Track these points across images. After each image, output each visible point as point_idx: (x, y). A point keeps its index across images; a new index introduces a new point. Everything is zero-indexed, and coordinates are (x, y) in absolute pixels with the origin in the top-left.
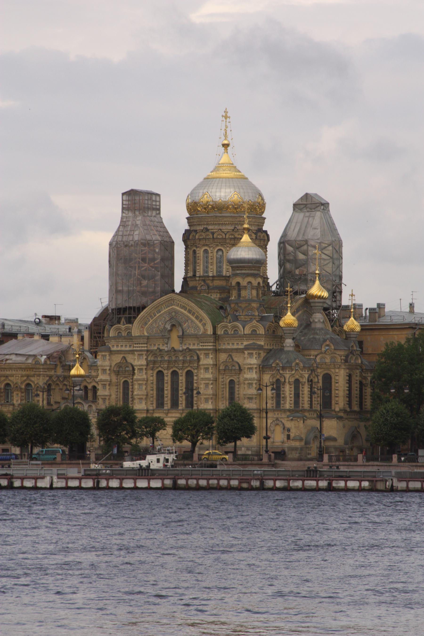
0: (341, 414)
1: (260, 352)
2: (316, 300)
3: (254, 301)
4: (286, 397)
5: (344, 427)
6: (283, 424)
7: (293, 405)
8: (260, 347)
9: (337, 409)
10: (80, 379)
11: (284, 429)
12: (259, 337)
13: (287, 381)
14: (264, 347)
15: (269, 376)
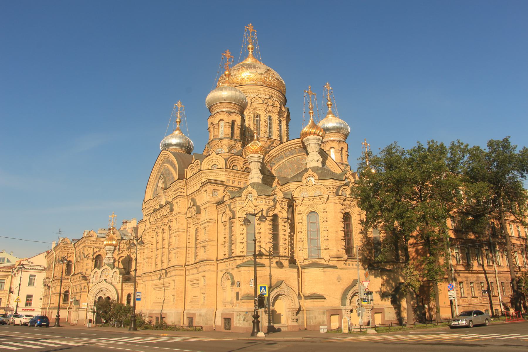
0: (333, 263)
1: (217, 188)
2: (309, 137)
3: (225, 138)
4: (236, 239)
5: (339, 279)
6: (233, 278)
7: (245, 250)
8: (220, 183)
9: (327, 257)
10: (109, 247)
11: (233, 284)
12: (219, 171)
13: (237, 216)
14: (226, 183)
15: (221, 215)
